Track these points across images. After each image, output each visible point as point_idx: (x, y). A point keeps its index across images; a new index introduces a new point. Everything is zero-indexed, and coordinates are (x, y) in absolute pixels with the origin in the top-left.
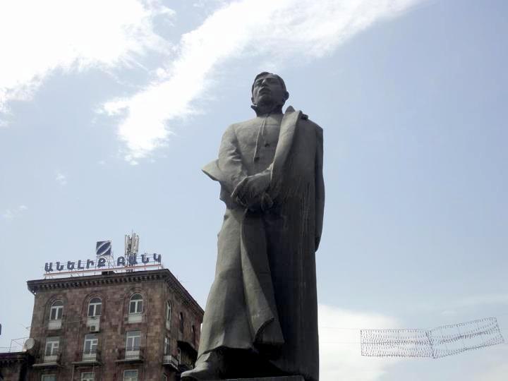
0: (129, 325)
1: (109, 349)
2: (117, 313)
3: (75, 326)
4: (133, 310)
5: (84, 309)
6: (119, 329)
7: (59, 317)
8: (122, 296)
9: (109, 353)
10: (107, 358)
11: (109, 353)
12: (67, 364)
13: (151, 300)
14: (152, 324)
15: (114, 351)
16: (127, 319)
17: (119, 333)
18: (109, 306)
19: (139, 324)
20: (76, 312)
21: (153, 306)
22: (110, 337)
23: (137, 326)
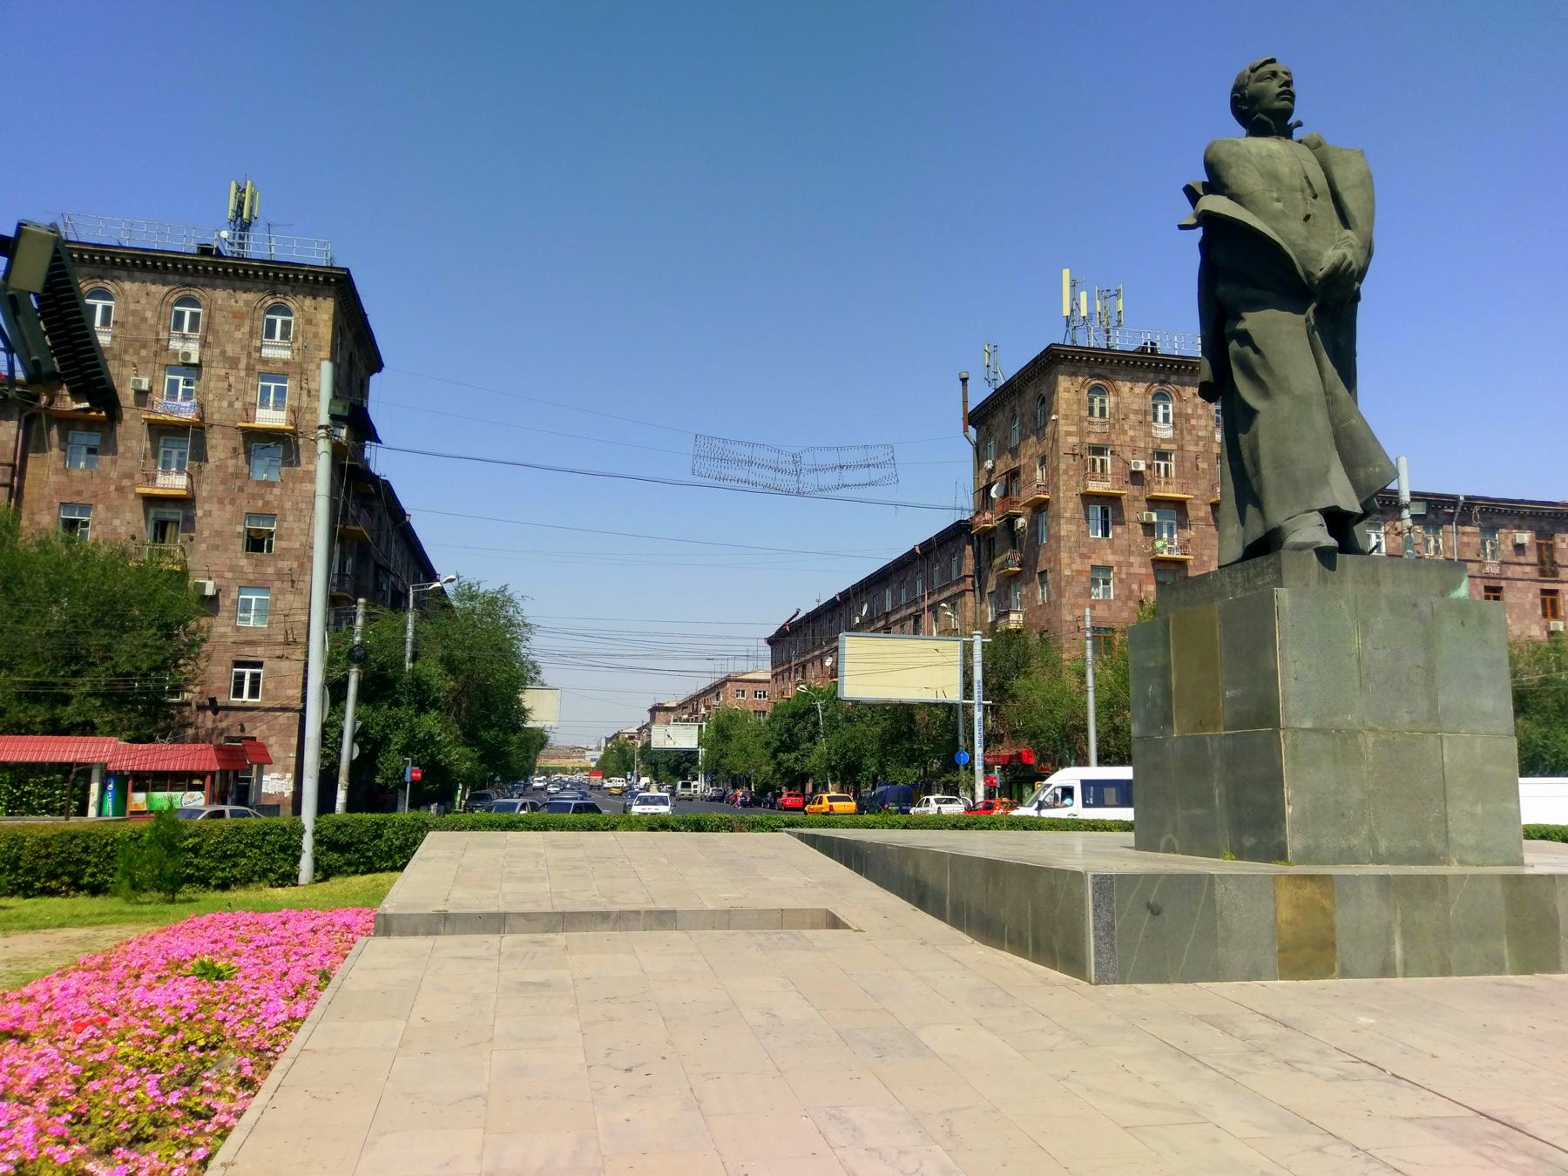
0: (266, 361)
2: (238, 335)
3: (144, 347)
4: (270, 333)
6: (242, 365)
8: (247, 303)
9: (220, 407)
10: (216, 416)
11: (220, 407)
13: (309, 322)
15: (231, 404)
16: (259, 350)
17: (243, 374)
18: (219, 317)
19: (286, 363)
20: (144, 320)
21: (316, 335)
23: (281, 365)
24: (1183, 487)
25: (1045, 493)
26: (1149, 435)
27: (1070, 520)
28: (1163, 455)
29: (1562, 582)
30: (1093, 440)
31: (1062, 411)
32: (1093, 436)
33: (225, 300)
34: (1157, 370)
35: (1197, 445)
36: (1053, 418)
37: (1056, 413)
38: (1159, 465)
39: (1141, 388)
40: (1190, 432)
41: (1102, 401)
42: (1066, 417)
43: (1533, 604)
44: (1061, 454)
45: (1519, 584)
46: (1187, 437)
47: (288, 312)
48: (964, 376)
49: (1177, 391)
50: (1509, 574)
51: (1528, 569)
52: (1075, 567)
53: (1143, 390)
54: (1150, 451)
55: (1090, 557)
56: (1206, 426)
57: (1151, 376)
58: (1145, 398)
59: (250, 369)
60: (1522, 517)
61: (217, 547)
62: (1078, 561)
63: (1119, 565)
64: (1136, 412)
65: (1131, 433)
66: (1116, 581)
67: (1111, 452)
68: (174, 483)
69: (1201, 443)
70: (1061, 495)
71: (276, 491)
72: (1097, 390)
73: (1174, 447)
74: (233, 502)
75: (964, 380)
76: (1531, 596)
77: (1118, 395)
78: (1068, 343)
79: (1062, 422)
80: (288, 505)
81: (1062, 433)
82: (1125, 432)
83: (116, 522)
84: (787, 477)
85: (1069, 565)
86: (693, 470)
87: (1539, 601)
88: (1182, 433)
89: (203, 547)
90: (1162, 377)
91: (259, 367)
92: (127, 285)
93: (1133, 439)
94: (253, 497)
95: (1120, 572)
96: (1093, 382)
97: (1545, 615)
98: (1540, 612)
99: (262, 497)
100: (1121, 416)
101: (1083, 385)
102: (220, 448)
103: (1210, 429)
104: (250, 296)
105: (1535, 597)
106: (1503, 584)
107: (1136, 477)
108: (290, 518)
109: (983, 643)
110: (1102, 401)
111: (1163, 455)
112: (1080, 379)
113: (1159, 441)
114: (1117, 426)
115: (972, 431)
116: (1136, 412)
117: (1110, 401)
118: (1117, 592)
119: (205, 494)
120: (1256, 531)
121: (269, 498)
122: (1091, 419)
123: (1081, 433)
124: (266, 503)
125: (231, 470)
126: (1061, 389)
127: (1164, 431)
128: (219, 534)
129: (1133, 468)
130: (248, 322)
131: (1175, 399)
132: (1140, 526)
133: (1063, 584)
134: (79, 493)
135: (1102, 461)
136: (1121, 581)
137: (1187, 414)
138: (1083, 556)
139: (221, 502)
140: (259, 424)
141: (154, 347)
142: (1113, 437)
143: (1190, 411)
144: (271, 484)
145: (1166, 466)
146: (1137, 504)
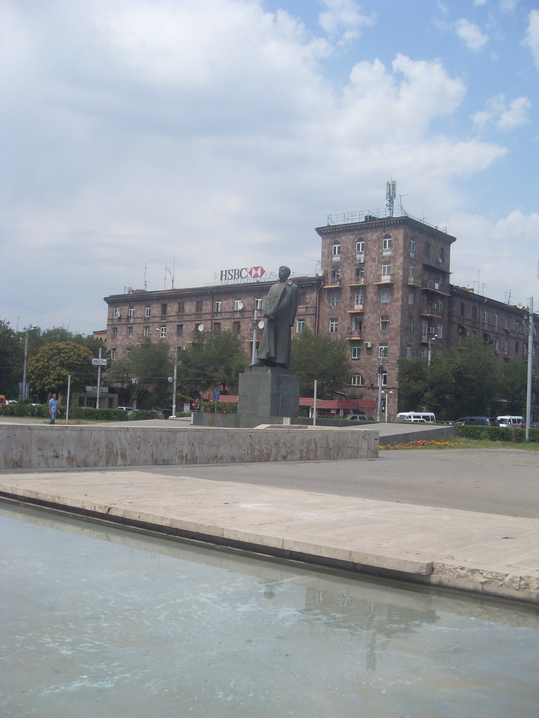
0: (383, 257)
1: (371, 275)
2: (375, 249)
3: (349, 259)
4: (385, 247)
5: (353, 247)
6: (377, 261)
7: (339, 253)
8: (377, 236)
9: (371, 277)
10: (370, 281)
11: (371, 277)
12: (345, 285)
14: (398, 257)
15: (374, 276)
16: (381, 253)
17: (377, 264)
18: (369, 243)
19: (390, 257)
20: (349, 249)
21: (398, 244)
22: (371, 266)
23: (388, 258)
33: (373, 236)
47: (390, 237)
59: (379, 261)
61: (372, 330)
68: (358, 307)
71: (388, 306)
74: (376, 312)
80: (392, 311)
83: (344, 323)
89: (368, 330)
91: (382, 260)
92: (343, 238)
94: (382, 309)
99: (384, 309)
102: (371, 294)
104: (377, 234)
108: (393, 316)
119: (368, 310)
121: (386, 309)
124: (386, 311)
125: (375, 300)
128: (372, 324)
130: (378, 244)
134: (334, 314)
139: (372, 313)
140: (383, 282)
141: (352, 259)
144: (386, 304)
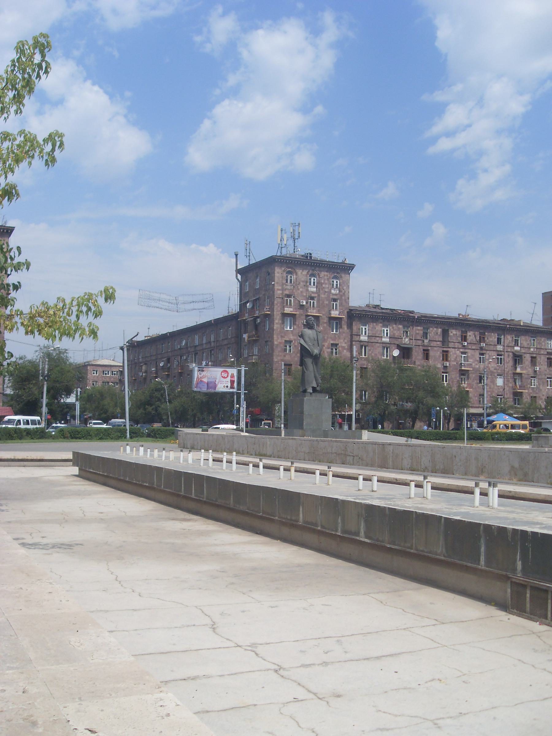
24: (319, 312)
25: (269, 311)
26: (307, 290)
27: (277, 323)
28: (312, 298)
29: (450, 348)
30: (287, 292)
31: (276, 281)
32: (287, 290)
34: (311, 266)
35: (325, 294)
36: (273, 283)
37: (274, 281)
38: (311, 302)
39: (305, 272)
40: (322, 289)
41: (291, 277)
42: (277, 283)
43: (439, 356)
44: (275, 297)
45: (435, 348)
46: (321, 292)
48: (237, 254)
49: (318, 273)
50: (432, 345)
51: (438, 343)
52: (279, 341)
53: (306, 273)
54: (308, 297)
55: (284, 337)
56: (328, 288)
57: (309, 268)
58: (307, 276)
60: (438, 324)
62: (280, 338)
63: (295, 340)
64: (303, 282)
65: (301, 290)
66: (293, 346)
67: (293, 297)
69: (326, 294)
70: (275, 313)
72: (289, 273)
73: (316, 295)
75: (236, 255)
76: (439, 353)
77: (296, 275)
78: (279, 254)
79: (276, 285)
81: (276, 290)
82: (299, 289)
84: (173, 305)
85: (277, 340)
86: (138, 303)
87: (441, 355)
88: (319, 290)
90: (313, 268)
93: (302, 292)
95: (295, 342)
96: (288, 270)
97: (443, 359)
98: (441, 359)
100: (298, 283)
101: (284, 271)
103: (330, 288)
105: (440, 352)
106: (429, 348)
107: (302, 306)
109: (245, 370)
110: (291, 277)
111: (312, 298)
112: (283, 269)
113: (311, 293)
114: (296, 287)
115: (239, 277)
116: (303, 282)
117: (294, 277)
118: (294, 351)
120: (304, 389)
122: (287, 284)
123: (283, 290)
126: (276, 272)
127: (313, 289)
129: (301, 304)
131: (317, 277)
132: (303, 325)
133: (274, 347)
135: (290, 300)
136: (295, 346)
137: (321, 283)
138: (282, 337)
142: (294, 291)
143: (323, 281)
145: (313, 302)
146: (302, 317)
